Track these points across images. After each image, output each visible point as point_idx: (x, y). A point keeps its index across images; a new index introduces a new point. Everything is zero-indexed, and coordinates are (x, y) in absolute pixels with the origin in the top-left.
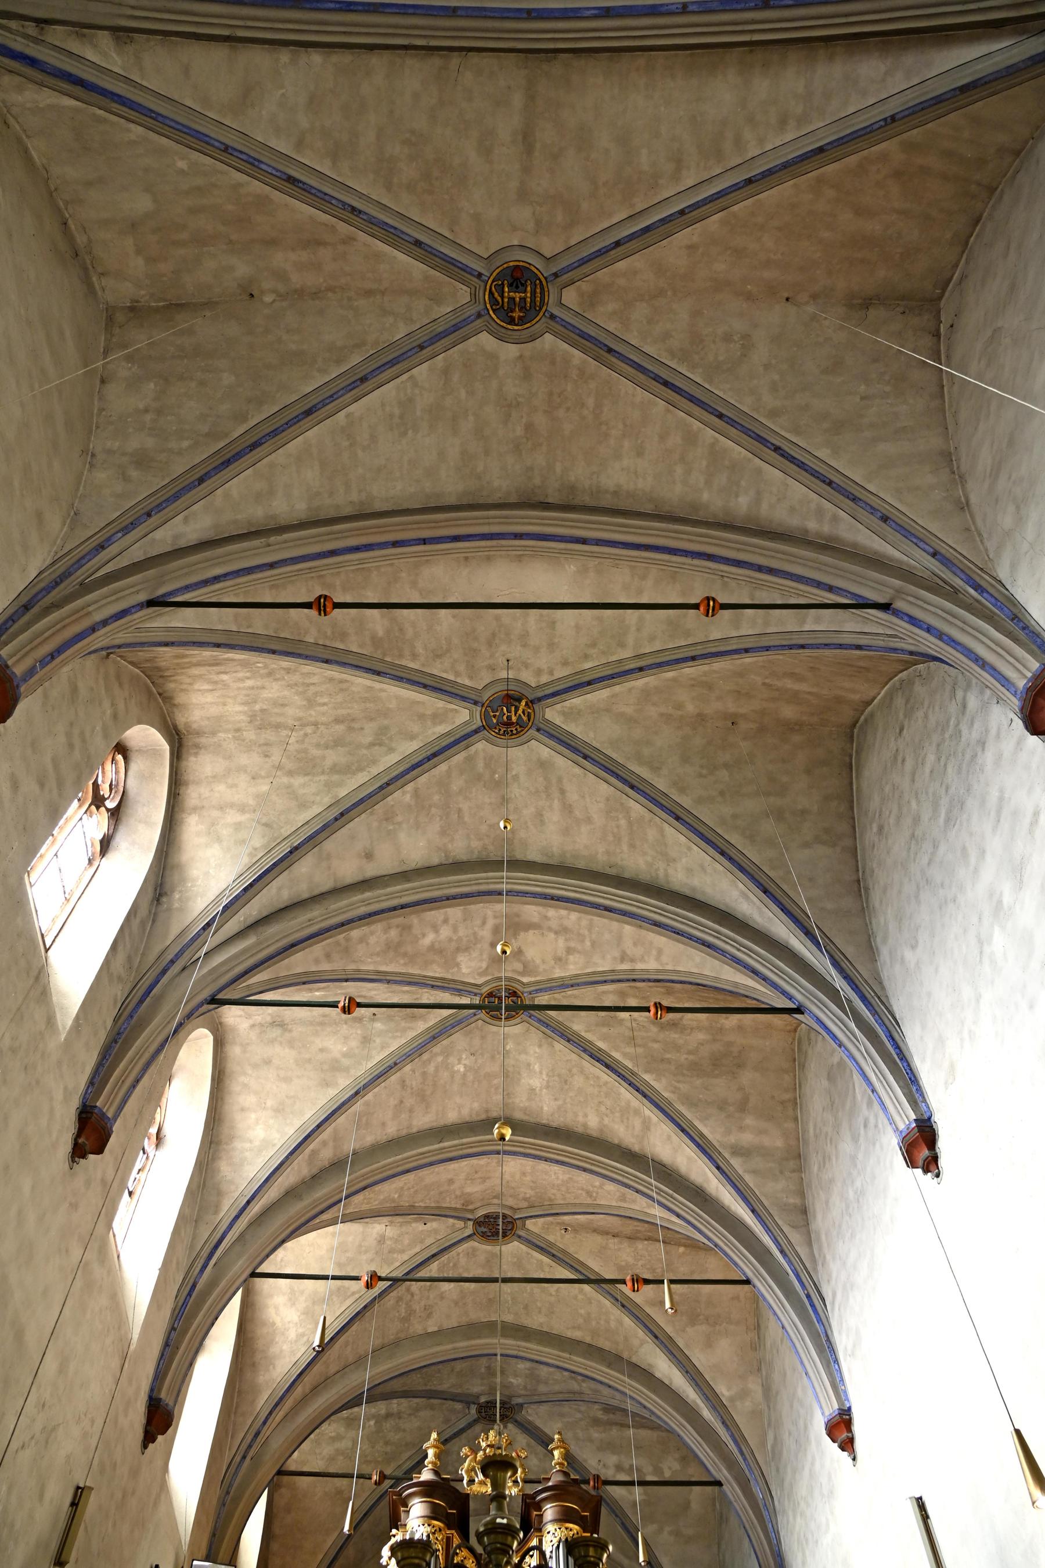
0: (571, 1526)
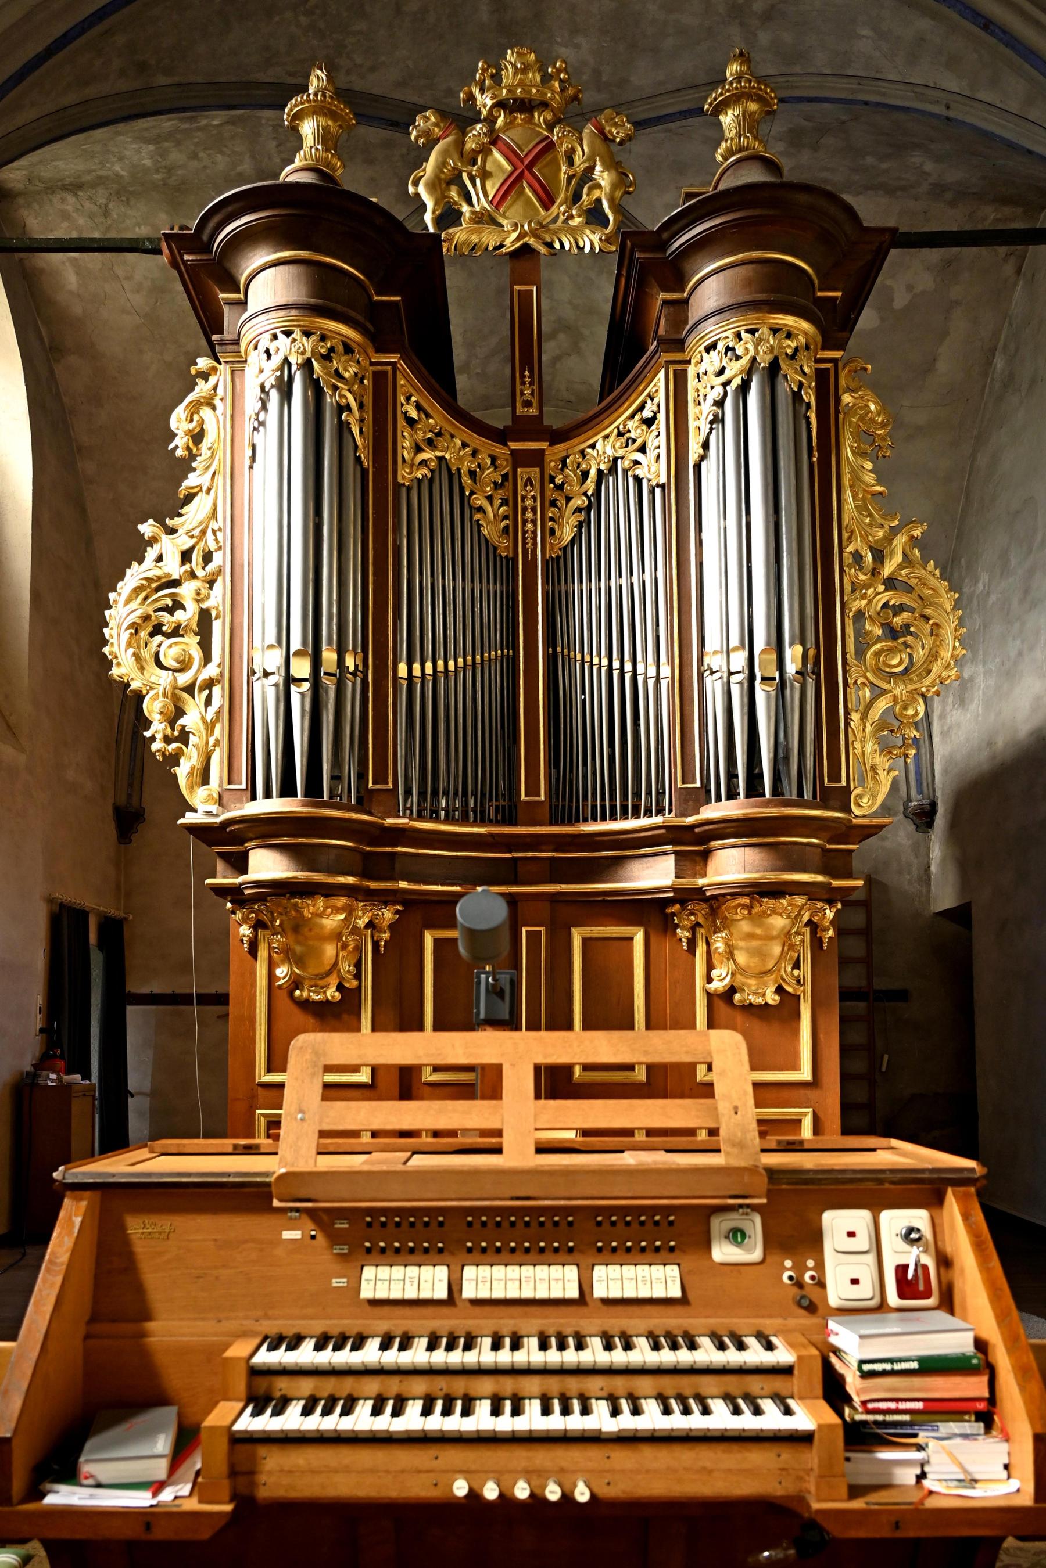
0: (789, 321)
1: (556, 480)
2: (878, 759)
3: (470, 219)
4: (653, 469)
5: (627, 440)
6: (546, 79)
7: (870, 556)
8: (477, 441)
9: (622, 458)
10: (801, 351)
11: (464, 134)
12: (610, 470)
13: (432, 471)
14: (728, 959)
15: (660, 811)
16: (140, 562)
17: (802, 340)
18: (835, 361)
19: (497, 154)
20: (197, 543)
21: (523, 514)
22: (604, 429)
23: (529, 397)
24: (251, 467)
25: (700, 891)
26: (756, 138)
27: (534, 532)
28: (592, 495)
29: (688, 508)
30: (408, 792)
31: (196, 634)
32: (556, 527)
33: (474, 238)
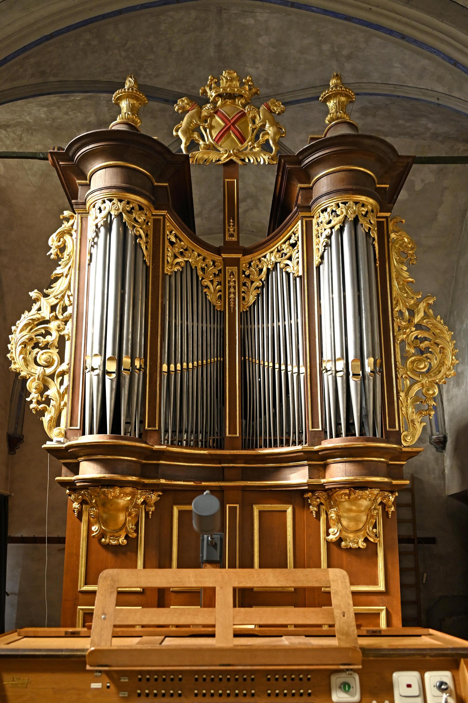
0: (363, 198)
1: (246, 273)
2: (415, 417)
3: (204, 147)
4: (295, 268)
5: (282, 254)
6: (242, 84)
7: (407, 313)
8: (205, 253)
9: (280, 263)
10: (369, 213)
11: (201, 108)
12: (273, 268)
13: (182, 268)
14: (338, 523)
15: (300, 443)
16: (29, 311)
17: (370, 208)
18: (386, 218)
19: (217, 118)
20: (59, 302)
21: (229, 289)
22: (270, 248)
23: (233, 232)
24: (89, 264)
25: (322, 486)
26: (345, 113)
27: (235, 299)
28: (264, 280)
29: (314, 288)
30: (166, 431)
31: (57, 348)
32: (246, 296)
33: (206, 157)
